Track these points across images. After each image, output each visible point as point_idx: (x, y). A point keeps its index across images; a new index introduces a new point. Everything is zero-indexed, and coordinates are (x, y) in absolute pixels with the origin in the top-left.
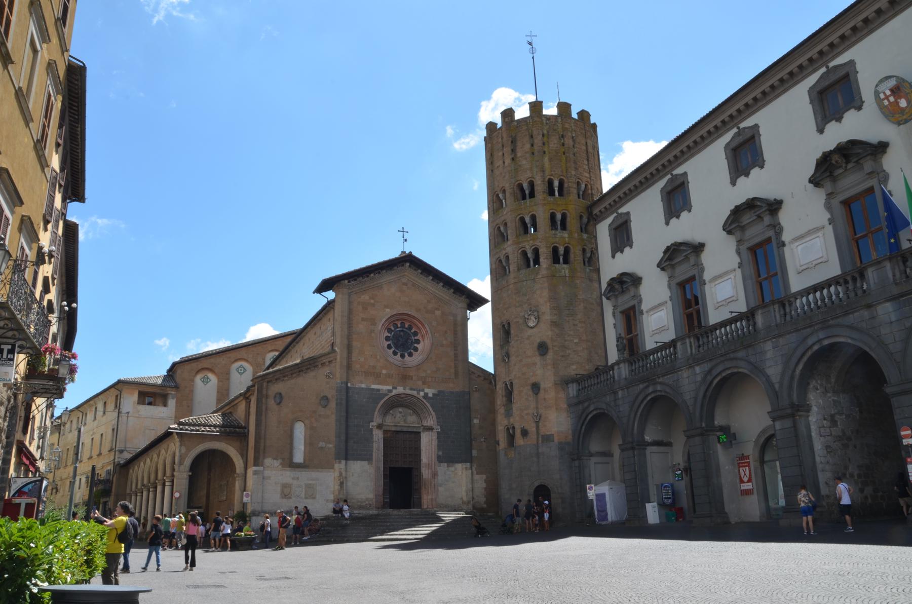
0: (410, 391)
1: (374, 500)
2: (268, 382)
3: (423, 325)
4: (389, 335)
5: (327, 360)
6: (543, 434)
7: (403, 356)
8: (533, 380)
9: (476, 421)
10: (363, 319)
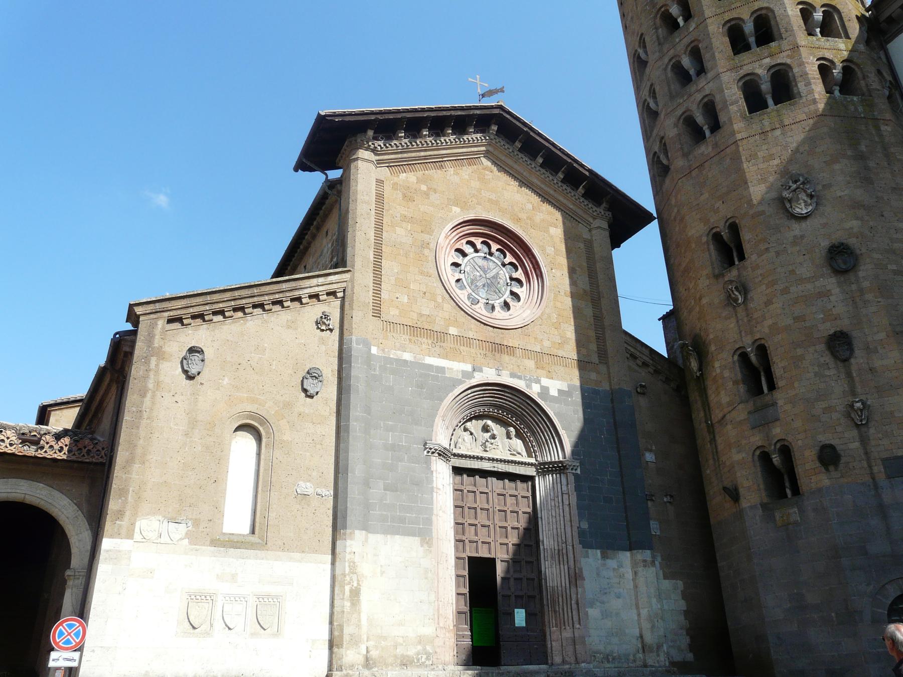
0: (512, 379)
2: (170, 321)
5: (321, 288)
6: (885, 455)
8: (829, 328)
9: (649, 457)
10: (404, 218)
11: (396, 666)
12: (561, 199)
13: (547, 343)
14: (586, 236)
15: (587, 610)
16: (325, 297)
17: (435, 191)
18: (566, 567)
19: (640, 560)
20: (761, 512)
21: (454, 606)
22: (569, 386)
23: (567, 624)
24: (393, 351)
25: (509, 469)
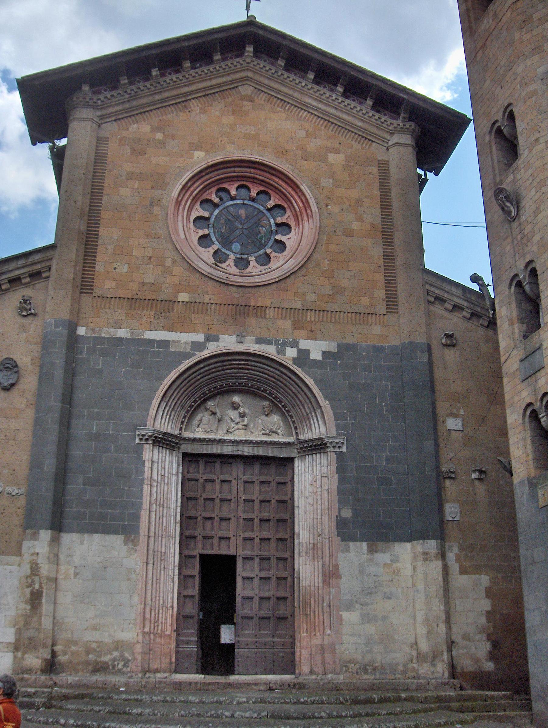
0: (257, 346)
1: (139, 648)
3: (296, 187)
4: (206, 214)
5: (22, 271)
7: (241, 263)
9: (453, 424)
10: (131, 176)
11: (87, 672)
12: (344, 116)
13: (311, 297)
14: (381, 156)
15: (341, 613)
16: (28, 280)
17: (173, 137)
18: (320, 563)
19: (419, 553)
20: (527, 488)
21: (175, 609)
22: (339, 346)
23: (317, 629)
24: (105, 330)
25: (258, 452)
